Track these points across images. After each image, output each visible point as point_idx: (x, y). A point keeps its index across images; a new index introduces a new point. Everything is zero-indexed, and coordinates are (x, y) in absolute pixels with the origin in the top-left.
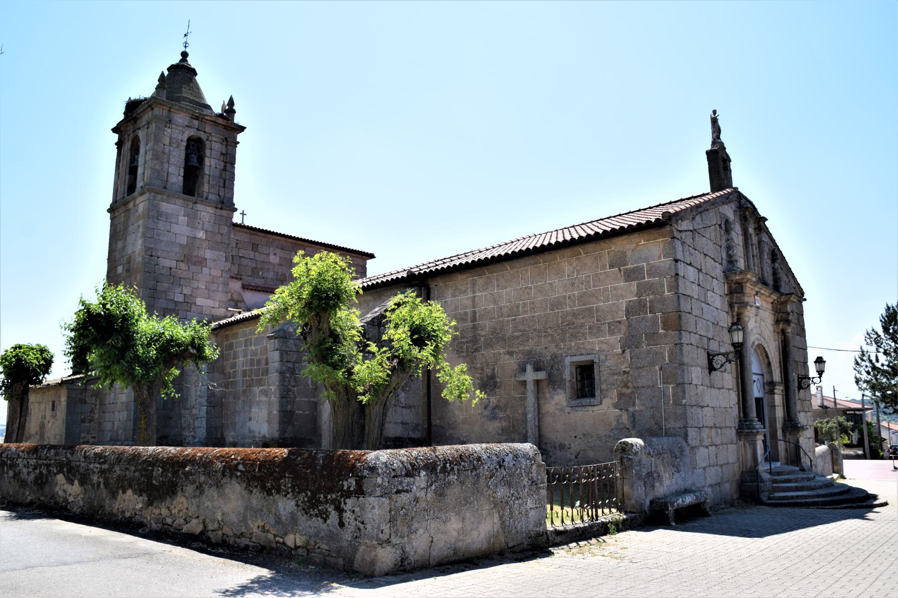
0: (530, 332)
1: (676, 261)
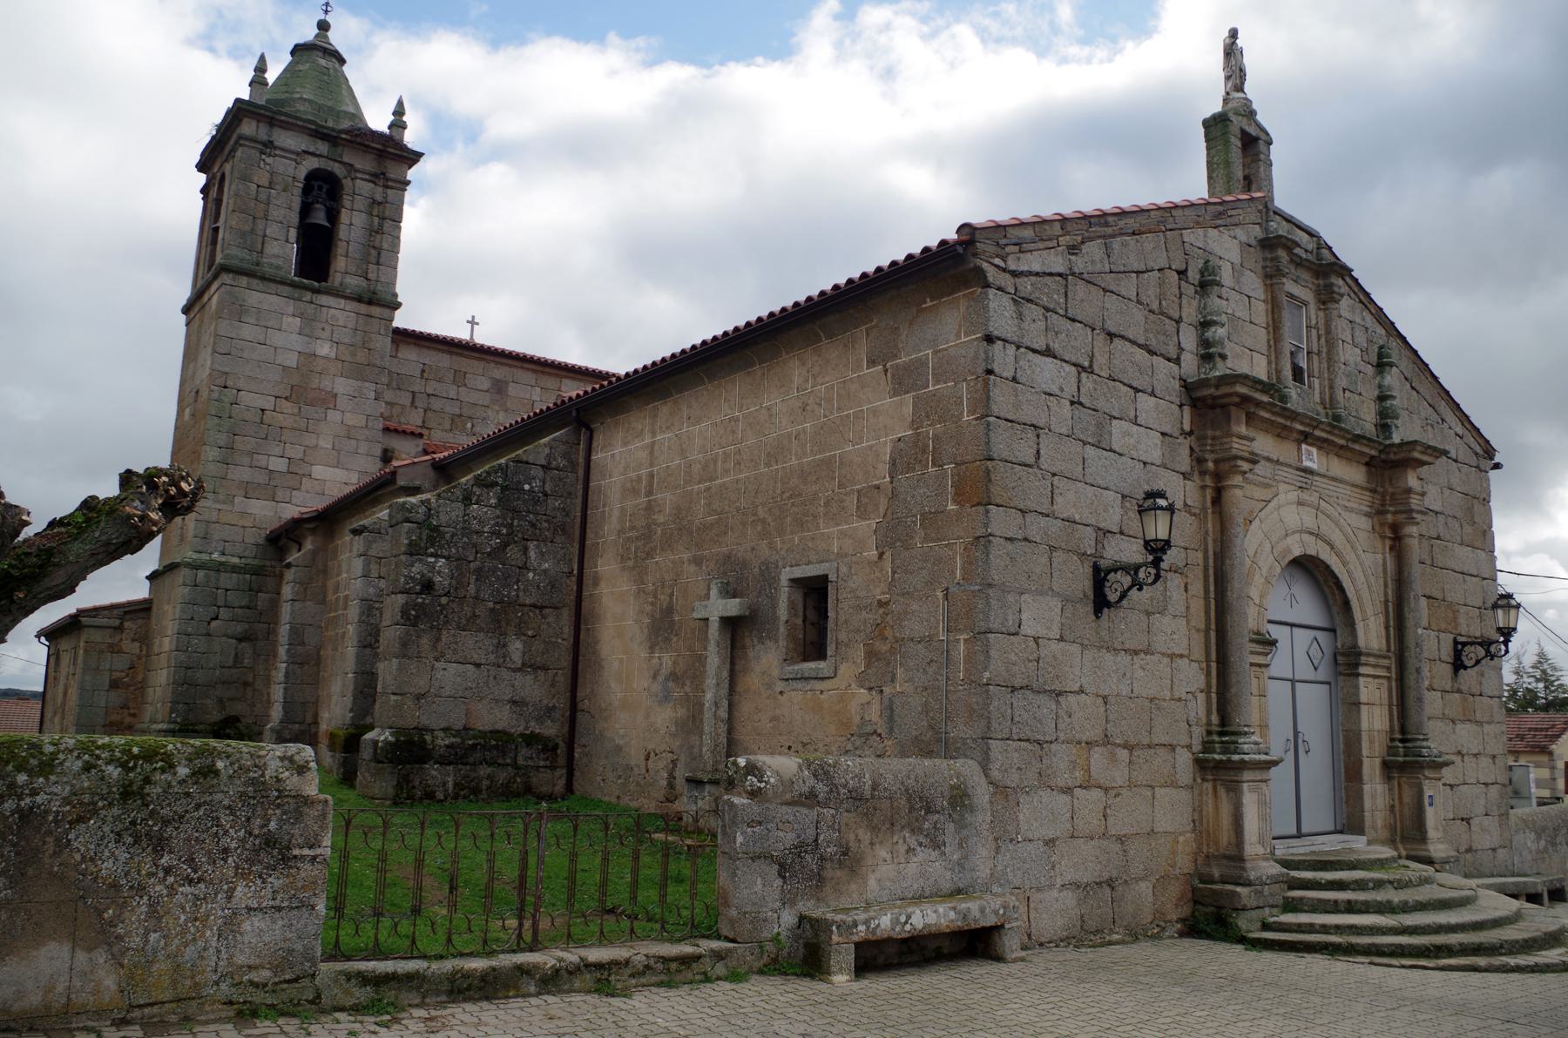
0: (730, 515)
1: (989, 339)
